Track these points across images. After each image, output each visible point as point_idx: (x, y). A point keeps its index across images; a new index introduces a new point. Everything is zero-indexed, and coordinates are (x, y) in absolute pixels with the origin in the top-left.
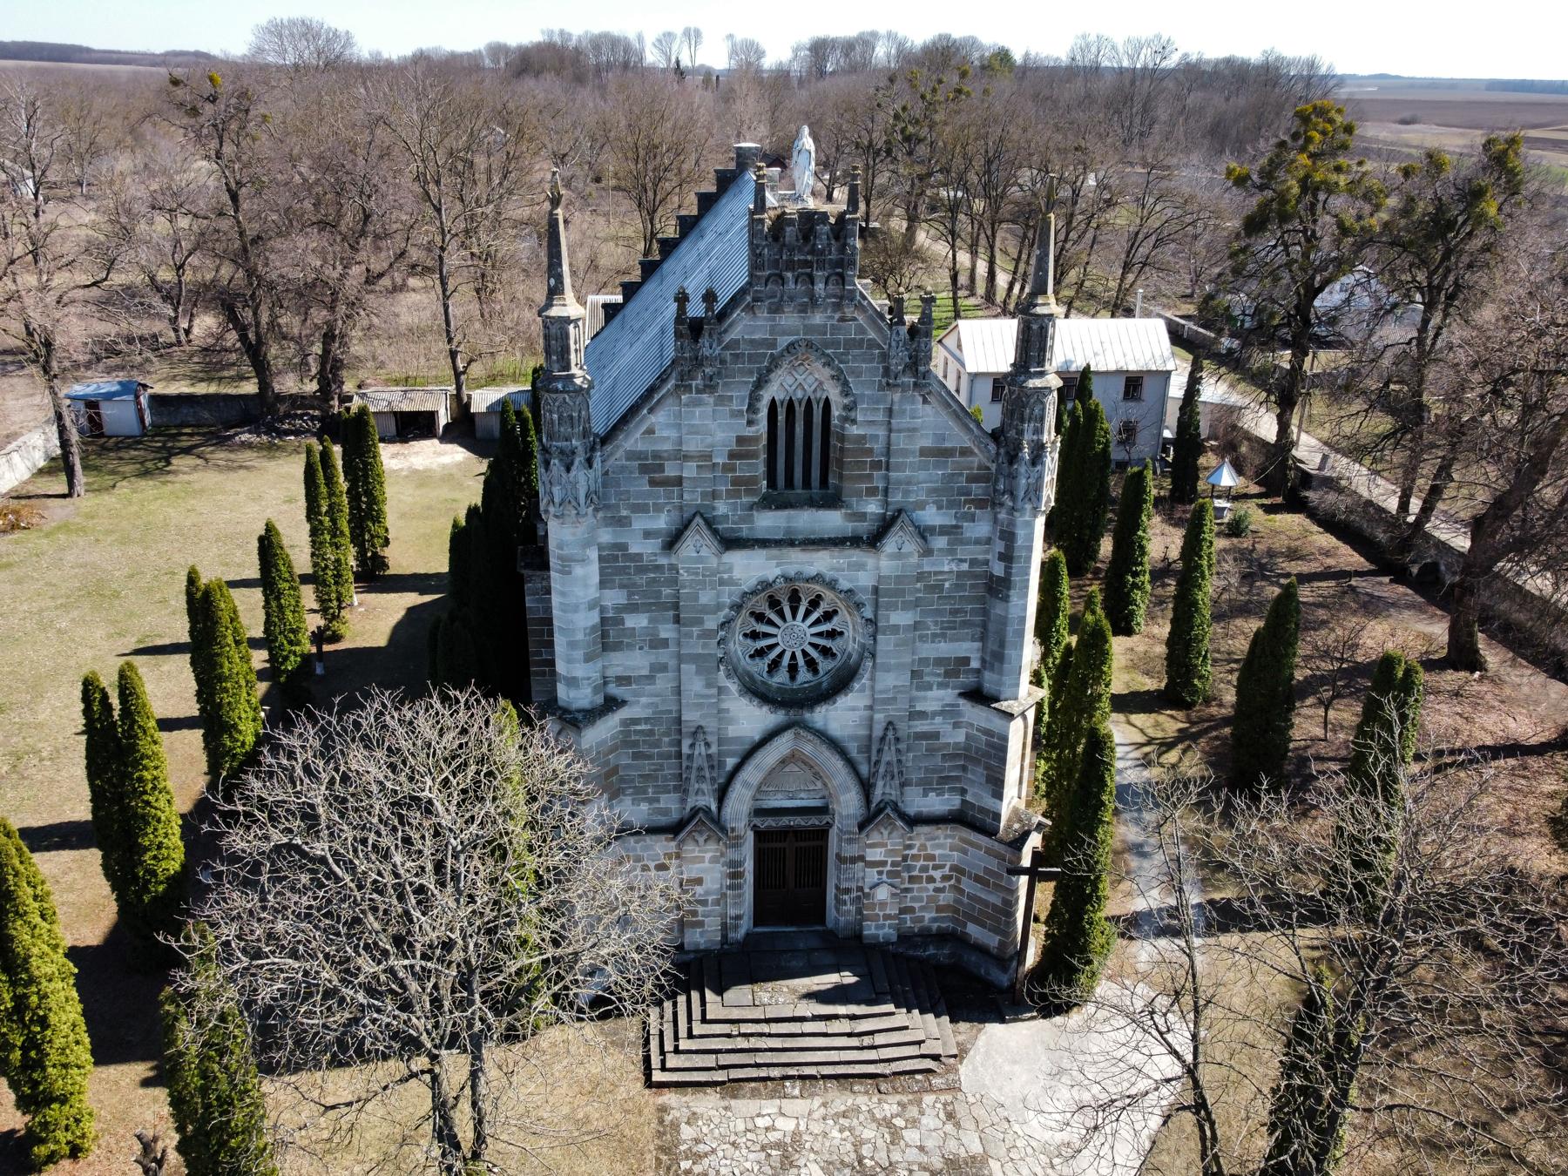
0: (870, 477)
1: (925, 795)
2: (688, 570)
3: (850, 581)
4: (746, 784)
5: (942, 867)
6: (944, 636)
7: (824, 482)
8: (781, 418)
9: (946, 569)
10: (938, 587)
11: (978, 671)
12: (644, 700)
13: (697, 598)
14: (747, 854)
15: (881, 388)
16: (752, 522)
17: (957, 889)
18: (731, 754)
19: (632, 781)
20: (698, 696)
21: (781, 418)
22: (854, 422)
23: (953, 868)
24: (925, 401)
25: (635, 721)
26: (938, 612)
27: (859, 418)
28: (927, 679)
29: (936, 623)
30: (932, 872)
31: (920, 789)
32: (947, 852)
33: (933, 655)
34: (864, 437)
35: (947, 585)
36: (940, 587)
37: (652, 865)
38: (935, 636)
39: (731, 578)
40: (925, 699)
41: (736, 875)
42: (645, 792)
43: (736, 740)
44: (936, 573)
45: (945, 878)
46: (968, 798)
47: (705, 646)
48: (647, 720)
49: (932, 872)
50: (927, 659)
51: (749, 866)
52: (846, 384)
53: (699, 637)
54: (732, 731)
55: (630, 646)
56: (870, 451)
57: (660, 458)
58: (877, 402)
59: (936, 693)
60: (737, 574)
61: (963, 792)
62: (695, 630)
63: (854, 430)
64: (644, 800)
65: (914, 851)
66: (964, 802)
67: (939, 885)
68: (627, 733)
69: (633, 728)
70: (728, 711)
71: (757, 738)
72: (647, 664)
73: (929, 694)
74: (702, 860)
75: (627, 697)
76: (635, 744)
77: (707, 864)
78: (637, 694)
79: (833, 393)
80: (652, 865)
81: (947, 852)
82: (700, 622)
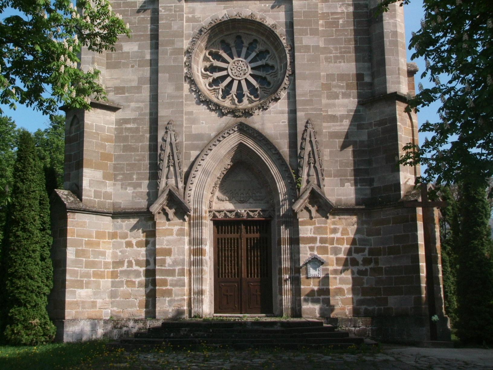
1: (343, 185)
2: (164, 8)
3: (274, 18)
4: (206, 173)
5: (363, 250)
6: (343, 57)
9: (339, 10)
10: (335, 23)
11: (371, 84)
12: (133, 105)
13: (170, 27)
14: (208, 232)
17: (376, 271)
18: (194, 148)
19: (122, 169)
20: (170, 97)
23: (371, 252)
25: (126, 121)
26: (336, 41)
28: (335, 90)
29: (336, 49)
30: (355, 255)
31: (337, 180)
32: (365, 236)
33: (336, 73)
35: (341, 21)
36: (335, 23)
37: (134, 242)
38: (336, 58)
39: (193, 17)
40: (334, 105)
41: (199, 252)
42: (132, 179)
43: (199, 137)
44: (333, 14)
45: (366, 261)
46: (376, 185)
47: (175, 60)
48: (135, 120)
49: (355, 255)
50: (333, 75)
51: (209, 249)
53: (172, 53)
54: (195, 129)
55: (125, 65)
59: (341, 101)
60: (197, 15)
61: (371, 181)
62: (169, 49)
64: (129, 185)
65: (339, 235)
66: (373, 190)
67: (362, 268)
68: (119, 131)
69: (124, 126)
70: (191, 113)
71: (213, 134)
72: (136, 78)
73: (337, 100)
74: (170, 232)
75: (122, 103)
76: (125, 139)
77: (175, 237)
78: (128, 100)
80: (134, 242)
81: (365, 236)
82: (173, 43)
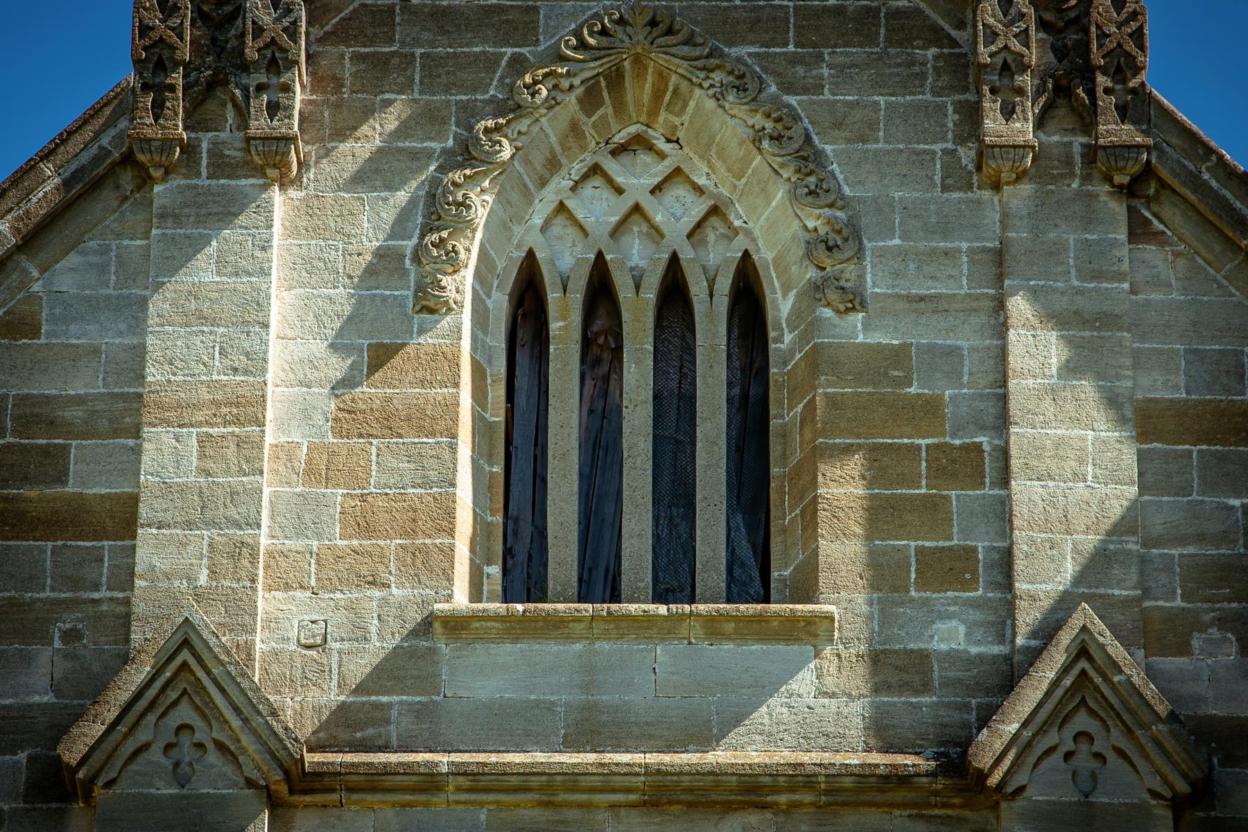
0: (934, 508)
7: (752, 575)
8: (565, 322)
15: (956, 179)
16: (430, 683)
21: (565, 322)
22: (854, 301)
24: (1139, 231)
27: (875, 285)
34: (898, 356)
52: (808, 159)
56: (929, 410)
57: (52, 425)
58: (945, 230)
63: (856, 331)
79: (773, 225)
